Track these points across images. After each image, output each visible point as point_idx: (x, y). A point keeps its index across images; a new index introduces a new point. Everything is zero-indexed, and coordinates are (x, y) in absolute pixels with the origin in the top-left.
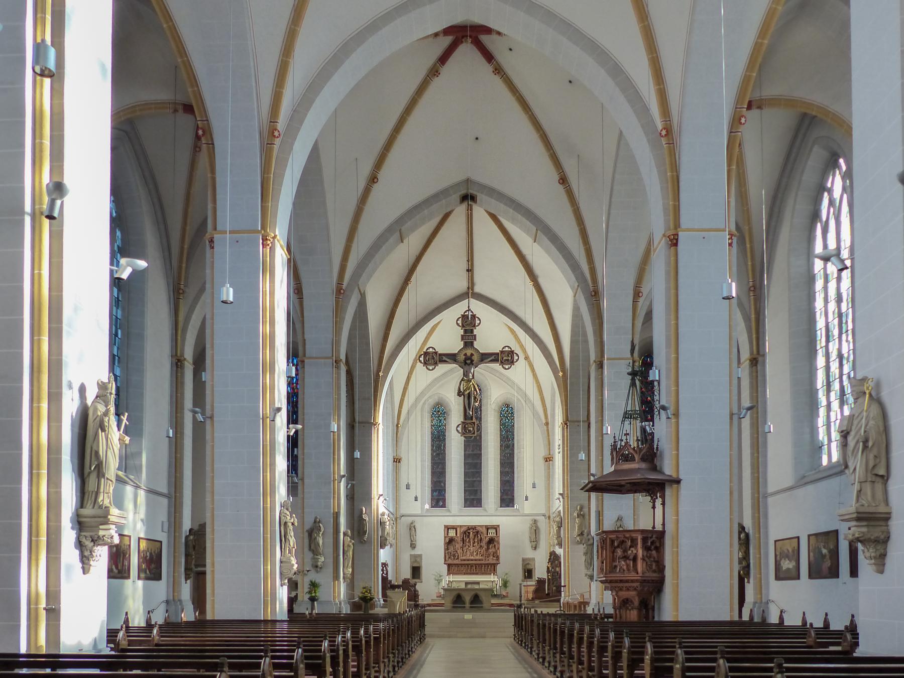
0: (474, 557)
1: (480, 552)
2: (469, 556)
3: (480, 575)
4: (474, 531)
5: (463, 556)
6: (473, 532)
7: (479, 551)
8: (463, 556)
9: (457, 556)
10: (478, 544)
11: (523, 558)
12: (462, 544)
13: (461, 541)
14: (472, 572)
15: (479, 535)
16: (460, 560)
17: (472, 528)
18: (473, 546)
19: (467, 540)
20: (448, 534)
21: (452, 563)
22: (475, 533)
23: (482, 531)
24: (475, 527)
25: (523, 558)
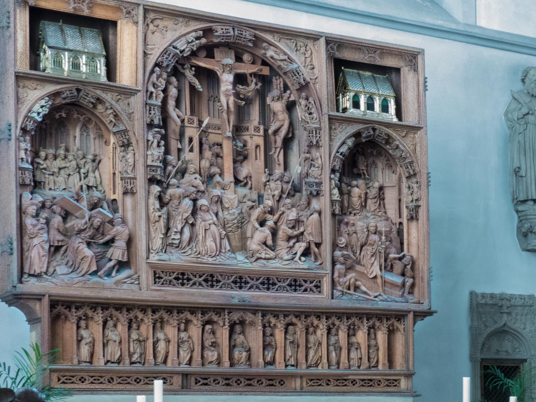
0: (253, 256)
1: (298, 222)
2: (220, 250)
3: (302, 392)
4: (246, 69)
5: (167, 246)
6: (240, 79)
7: (292, 215)
8: (167, 246)
9: (121, 243)
10: (268, 163)
11: (472, 294)
12: (157, 152)
13: (150, 126)
14: (241, 369)
15: (278, 106)
16: (146, 276)
17: (227, 45)
18: (237, 181)
19: (191, 132)
20: (35, 64)
21: (87, 293)
22: (253, 86)
23: (306, 73)
24: (257, 41)
25: (472, 294)
